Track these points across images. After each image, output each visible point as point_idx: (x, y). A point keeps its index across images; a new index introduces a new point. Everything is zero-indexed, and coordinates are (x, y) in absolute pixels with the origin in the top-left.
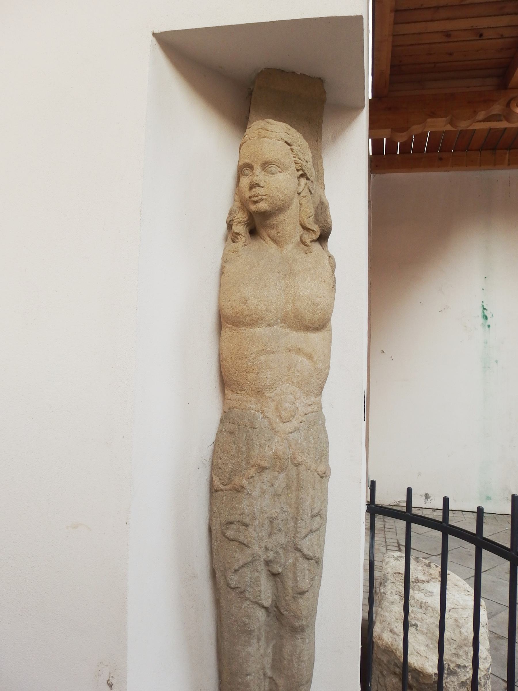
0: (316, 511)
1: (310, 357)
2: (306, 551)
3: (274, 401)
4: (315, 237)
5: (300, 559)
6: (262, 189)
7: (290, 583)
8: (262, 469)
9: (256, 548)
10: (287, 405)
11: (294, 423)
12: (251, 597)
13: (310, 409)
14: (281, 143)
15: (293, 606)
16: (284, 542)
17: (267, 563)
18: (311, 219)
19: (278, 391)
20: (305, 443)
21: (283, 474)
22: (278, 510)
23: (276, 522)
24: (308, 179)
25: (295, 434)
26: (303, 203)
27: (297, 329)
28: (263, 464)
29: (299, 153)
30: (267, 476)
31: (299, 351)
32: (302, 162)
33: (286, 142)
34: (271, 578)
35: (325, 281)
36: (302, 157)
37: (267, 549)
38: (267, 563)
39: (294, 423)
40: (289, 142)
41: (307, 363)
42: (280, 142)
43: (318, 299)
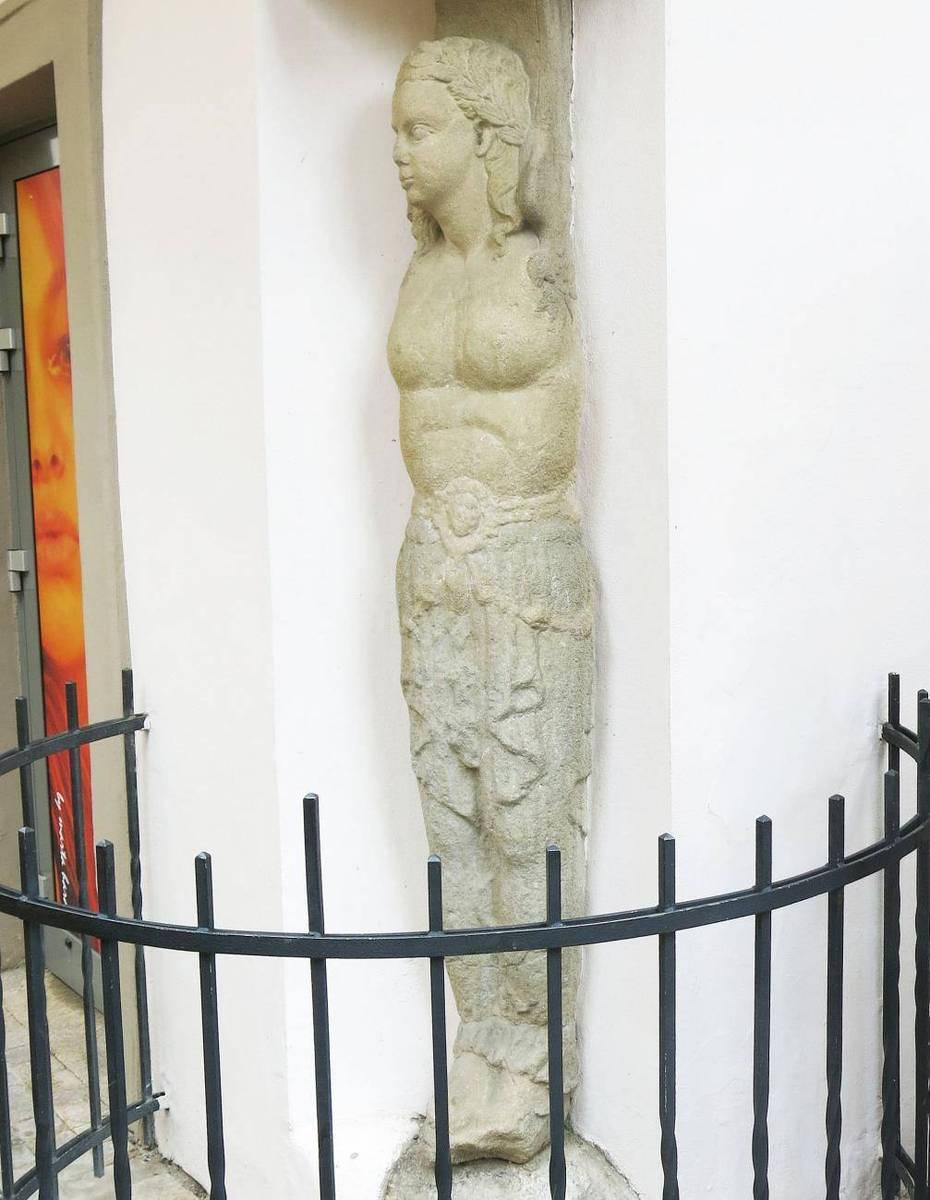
0: (522, 679)
1: (500, 433)
2: (507, 741)
3: (446, 502)
4: (509, 227)
5: (501, 751)
6: (407, 167)
7: (488, 785)
8: (429, 606)
9: (433, 723)
10: (462, 509)
11: (476, 539)
12: (436, 795)
13: (509, 516)
14: (431, 83)
15: (498, 822)
16: (473, 720)
17: (455, 748)
18: (511, 194)
19: (450, 488)
20: (495, 570)
21: (462, 620)
22: (459, 670)
23: (458, 687)
24: (495, 126)
25: (479, 556)
26: (492, 170)
27: (479, 388)
28: (431, 598)
29: (464, 90)
30: (440, 616)
31: (481, 423)
32: (473, 103)
33: (438, 80)
34: (469, 775)
35: (517, 305)
36: (473, 95)
37: (449, 727)
38: (455, 748)
39: (476, 539)
40: (442, 78)
41: (494, 440)
42: (428, 81)
43: (501, 337)
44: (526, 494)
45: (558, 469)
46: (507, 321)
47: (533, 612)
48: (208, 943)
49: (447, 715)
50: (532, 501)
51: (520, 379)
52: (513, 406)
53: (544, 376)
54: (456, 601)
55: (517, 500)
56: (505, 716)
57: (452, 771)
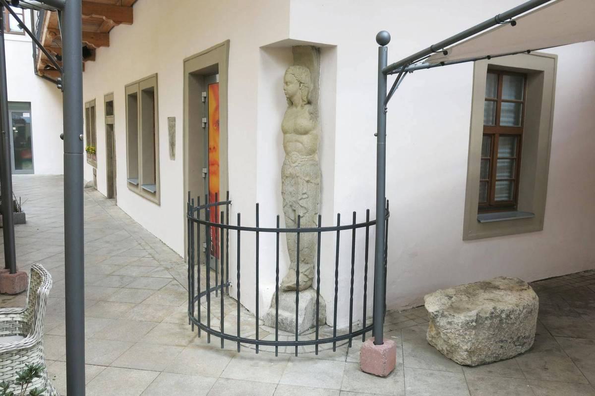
0: (304, 192)
1: (302, 143)
4: (305, 103)
9: (287, 201)
11: (296, 164)
13: (303, 160)
17: (291, 206)
18: (305, 97)
25: (297, 168)
38: (291, 206)
39: (296, 164)
44: (306, 156)
45: (313, 151)
46: (304, 121)
47: (307, 179)
48: (239, 229)
49: (290, 199)
50: (308, 157)
51: (306, 133)
52: (305, 138)
53: (311, 132)
54: (292, 176)
55: (305, 157)
56: (301, 199)
57: (290, 211)
